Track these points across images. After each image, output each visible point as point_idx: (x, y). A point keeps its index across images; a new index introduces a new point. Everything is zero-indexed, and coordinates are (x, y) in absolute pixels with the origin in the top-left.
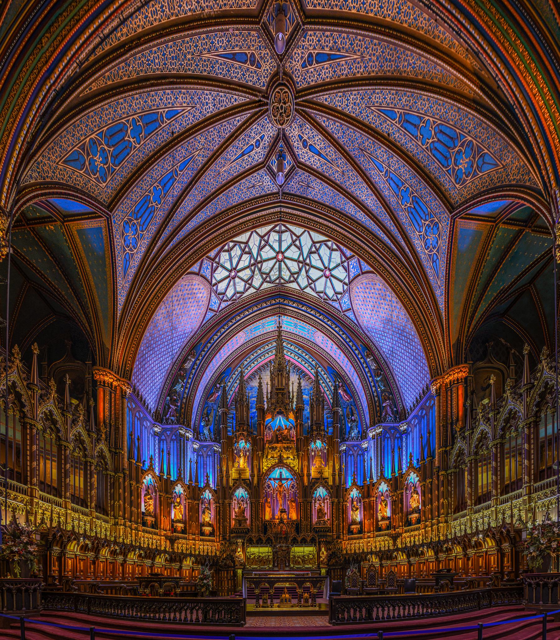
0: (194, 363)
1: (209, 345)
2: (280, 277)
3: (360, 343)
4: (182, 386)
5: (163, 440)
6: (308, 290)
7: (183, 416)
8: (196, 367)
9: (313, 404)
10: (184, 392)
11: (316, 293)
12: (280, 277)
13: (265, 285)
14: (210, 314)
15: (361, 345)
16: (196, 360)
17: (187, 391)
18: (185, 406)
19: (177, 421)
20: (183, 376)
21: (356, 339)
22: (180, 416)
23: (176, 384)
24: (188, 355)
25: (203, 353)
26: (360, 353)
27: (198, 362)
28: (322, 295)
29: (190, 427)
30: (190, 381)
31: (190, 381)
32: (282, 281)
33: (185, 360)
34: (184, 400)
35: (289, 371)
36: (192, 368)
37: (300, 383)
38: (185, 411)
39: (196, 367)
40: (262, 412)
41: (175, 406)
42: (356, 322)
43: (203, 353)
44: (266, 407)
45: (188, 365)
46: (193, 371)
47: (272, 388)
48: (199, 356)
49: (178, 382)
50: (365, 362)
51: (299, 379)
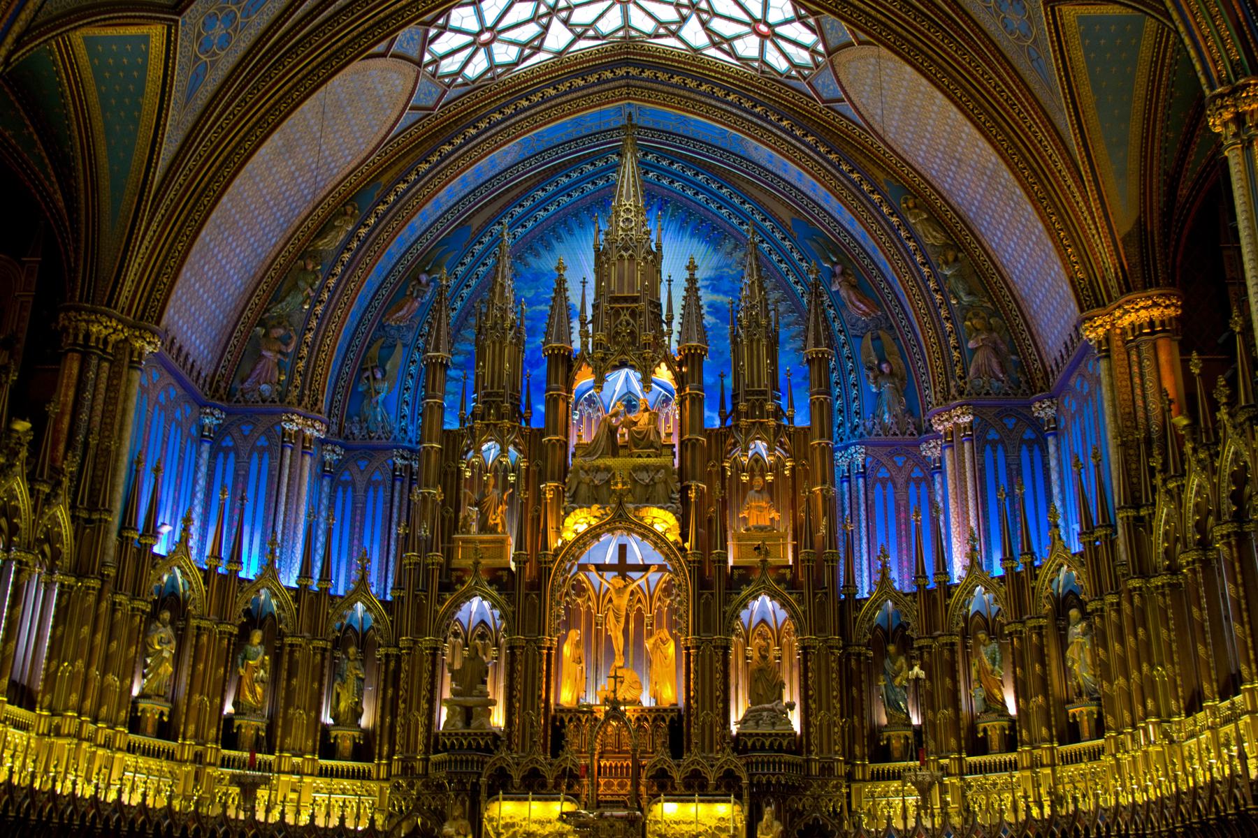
0: (352, 235)
1: (403, 186)
2: (626, 25)
3: (881, 176)
4: (308, 296)
5: (227, 451)
6: (713, 52)
7: (298, 381)
8: (355, 245)
9: (738, 335)
10: (311, 312)
11: (738, 59)
12: (626, 25)
13: (582, 44)
14: (409, 117)
15: (887, 182)
16: (357, 227)
17: (319, 309)
18: (310, 353)
19: (280, 394)
20: (314, 272)
21: (870, 166)
22: (291, 380)
23: (287, 295)
24: (335, 217)
25: (382, 208)
26: (885, 199)
27: (363, 232)
28: (756, 64)
29: (319, 412)
30: (332, 282)
31: (332, 282)
32: (633, 33)
33: (323, 229)
34: (310, 336)
35: (659, 247)
36: (345, 247)
37: (692, 281)
38: (307, 367)
39: (355, 245)
40: (566, 363)
41: (280, 352)
42: (860, 121)
43: (382, 208)
44: (577, 345)
45: (329, 244)
46: (347, 256)
47: (598, 295)
48: (369, 217)
49: (295, 286)
50: (904, 223)
51: (692, 267)
